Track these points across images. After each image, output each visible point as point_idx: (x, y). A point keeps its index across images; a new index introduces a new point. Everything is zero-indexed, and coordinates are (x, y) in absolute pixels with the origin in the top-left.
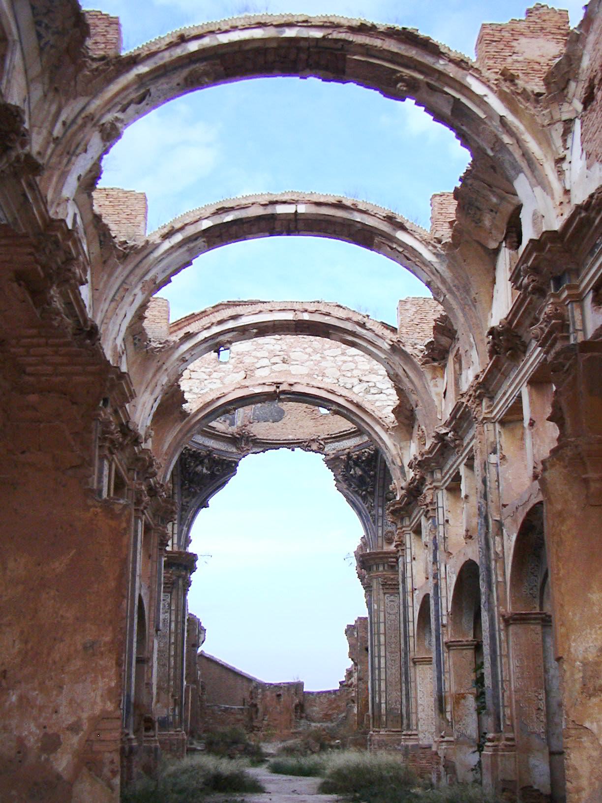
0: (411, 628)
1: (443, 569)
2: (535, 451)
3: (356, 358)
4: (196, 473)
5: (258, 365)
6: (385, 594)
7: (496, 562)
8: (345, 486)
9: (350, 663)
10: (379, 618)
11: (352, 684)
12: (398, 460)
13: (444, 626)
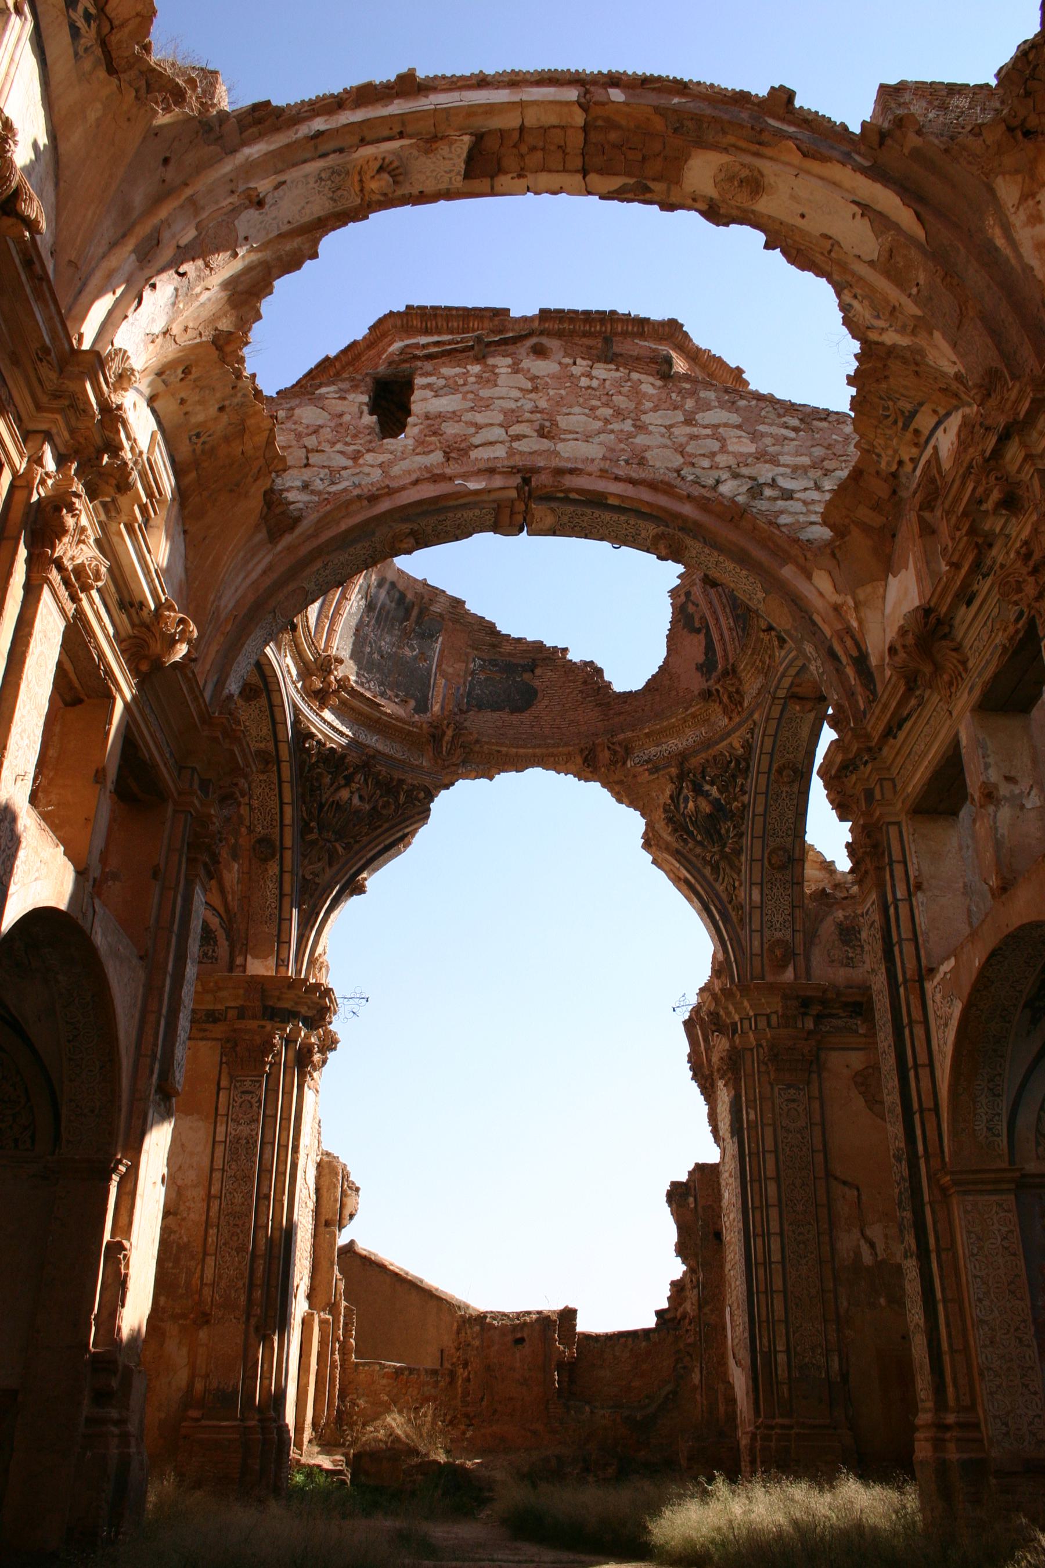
3: (721, 430)
4: (338, 806)
5: (476, 440)
9: (677, 1269)
11: (684, 1316)
12: (849, 643)
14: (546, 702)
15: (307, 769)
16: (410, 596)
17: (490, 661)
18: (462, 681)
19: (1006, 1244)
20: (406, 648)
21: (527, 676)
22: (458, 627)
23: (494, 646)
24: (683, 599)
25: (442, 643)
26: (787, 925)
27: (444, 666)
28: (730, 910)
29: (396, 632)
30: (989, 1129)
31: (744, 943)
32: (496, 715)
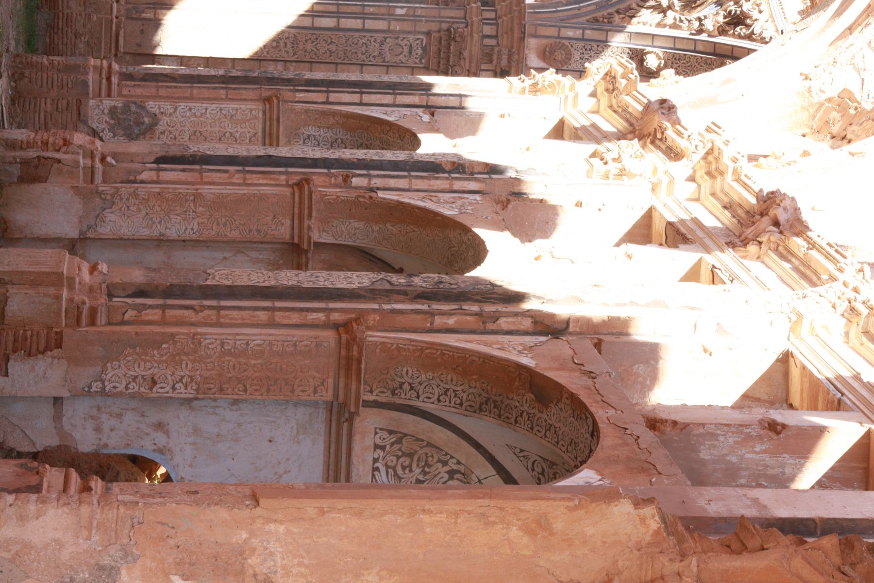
0: (346, 98)
1: (473, 186)
2: (711, 429)
6: (428, 34)
7: (479, 314)
10: (375, 17)
13: (346, 178)
19: (228, 135)
30: (309, 136)
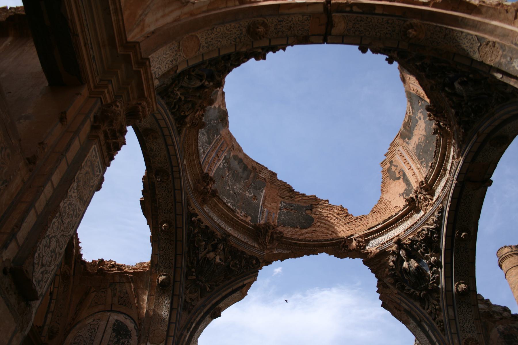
8: (396, 291)
14: (319, 224)
15: (192, 236)
16: (250, 167)
17: (289, 204)
18: (275, 211)
20: (247, 192)
21: (308, 212)
22: (273, 186)
23: (291, 197)
24: (388, 165)
25: (265, 193)
26: (473, 328)
27: (266, 204)
28: (435, 324)
29: (242, 183)
31: (447, 342)
32: (293, 229)
